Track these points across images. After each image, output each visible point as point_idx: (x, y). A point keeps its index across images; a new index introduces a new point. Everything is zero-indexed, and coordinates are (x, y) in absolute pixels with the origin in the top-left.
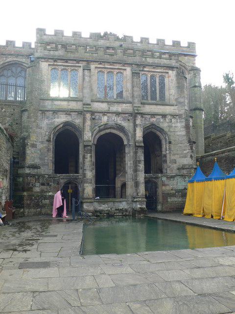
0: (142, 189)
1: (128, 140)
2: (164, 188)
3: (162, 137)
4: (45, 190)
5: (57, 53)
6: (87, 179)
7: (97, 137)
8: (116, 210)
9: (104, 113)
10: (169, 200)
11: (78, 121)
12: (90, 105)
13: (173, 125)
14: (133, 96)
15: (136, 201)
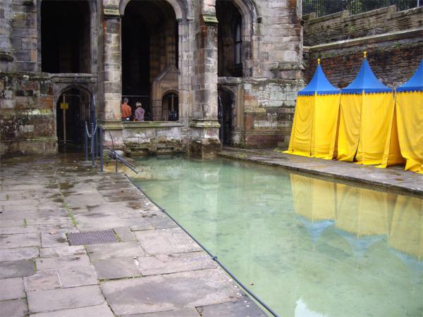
0: (212, 106)
4: (25, 105)
6: (111, 84)
8: (161, 142)
10: (256, 125)
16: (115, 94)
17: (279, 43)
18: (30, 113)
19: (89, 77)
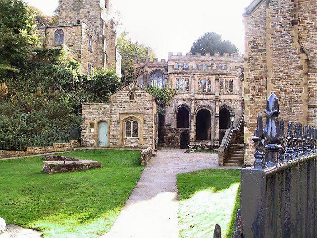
5: (179, 71)
11: (187, 103)
12: (193, 96)
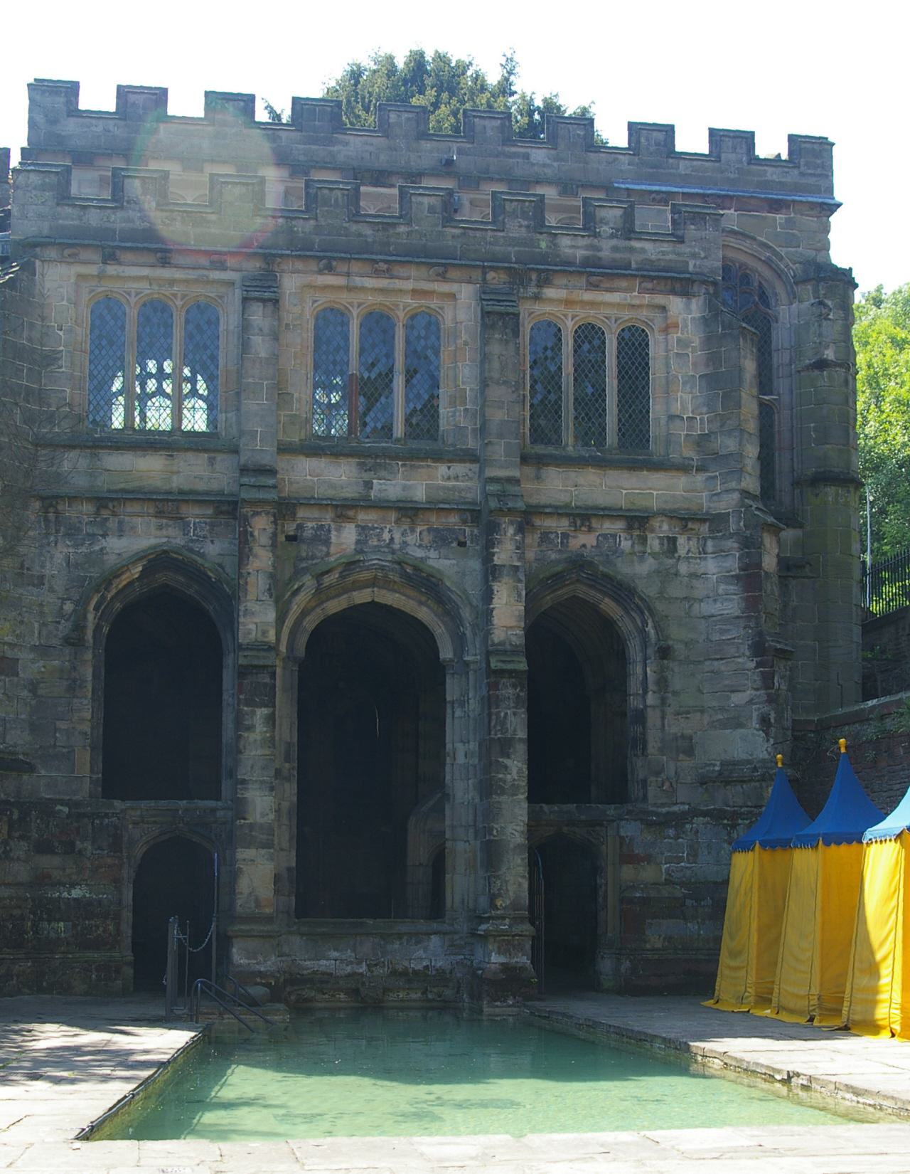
1: (460, 642)
2: (627, 872)
3: (626, 625)
6: (251, 826)
7: (310, 623)
8: (394, 973)
9: (343, 509)
11: (214, 550)
13: (683, 568)
14: (483, 430)
15: (484, 938)
16: (263, 851)
17: (722, 709)
18: (65, 895)
19: (213, 810)
